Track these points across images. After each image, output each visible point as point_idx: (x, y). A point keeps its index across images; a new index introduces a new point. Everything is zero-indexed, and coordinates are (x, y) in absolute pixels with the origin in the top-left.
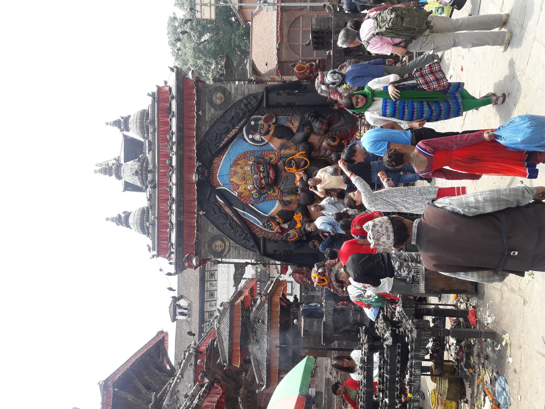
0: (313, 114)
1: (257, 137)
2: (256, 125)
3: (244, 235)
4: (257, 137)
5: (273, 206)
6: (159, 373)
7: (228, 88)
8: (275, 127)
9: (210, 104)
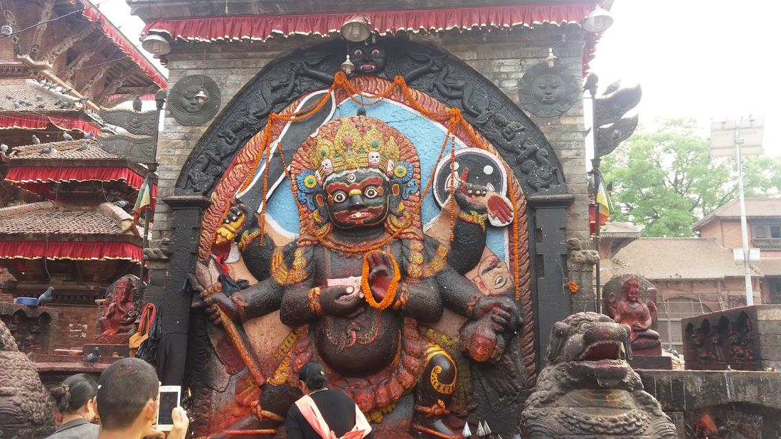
0: (513, 319)
1: (454, 181)
2: (485, 179)
3: (218, 158)
5: (285, 226)
6: (96, 80)
7: (571, 111)
8: (479, 224)
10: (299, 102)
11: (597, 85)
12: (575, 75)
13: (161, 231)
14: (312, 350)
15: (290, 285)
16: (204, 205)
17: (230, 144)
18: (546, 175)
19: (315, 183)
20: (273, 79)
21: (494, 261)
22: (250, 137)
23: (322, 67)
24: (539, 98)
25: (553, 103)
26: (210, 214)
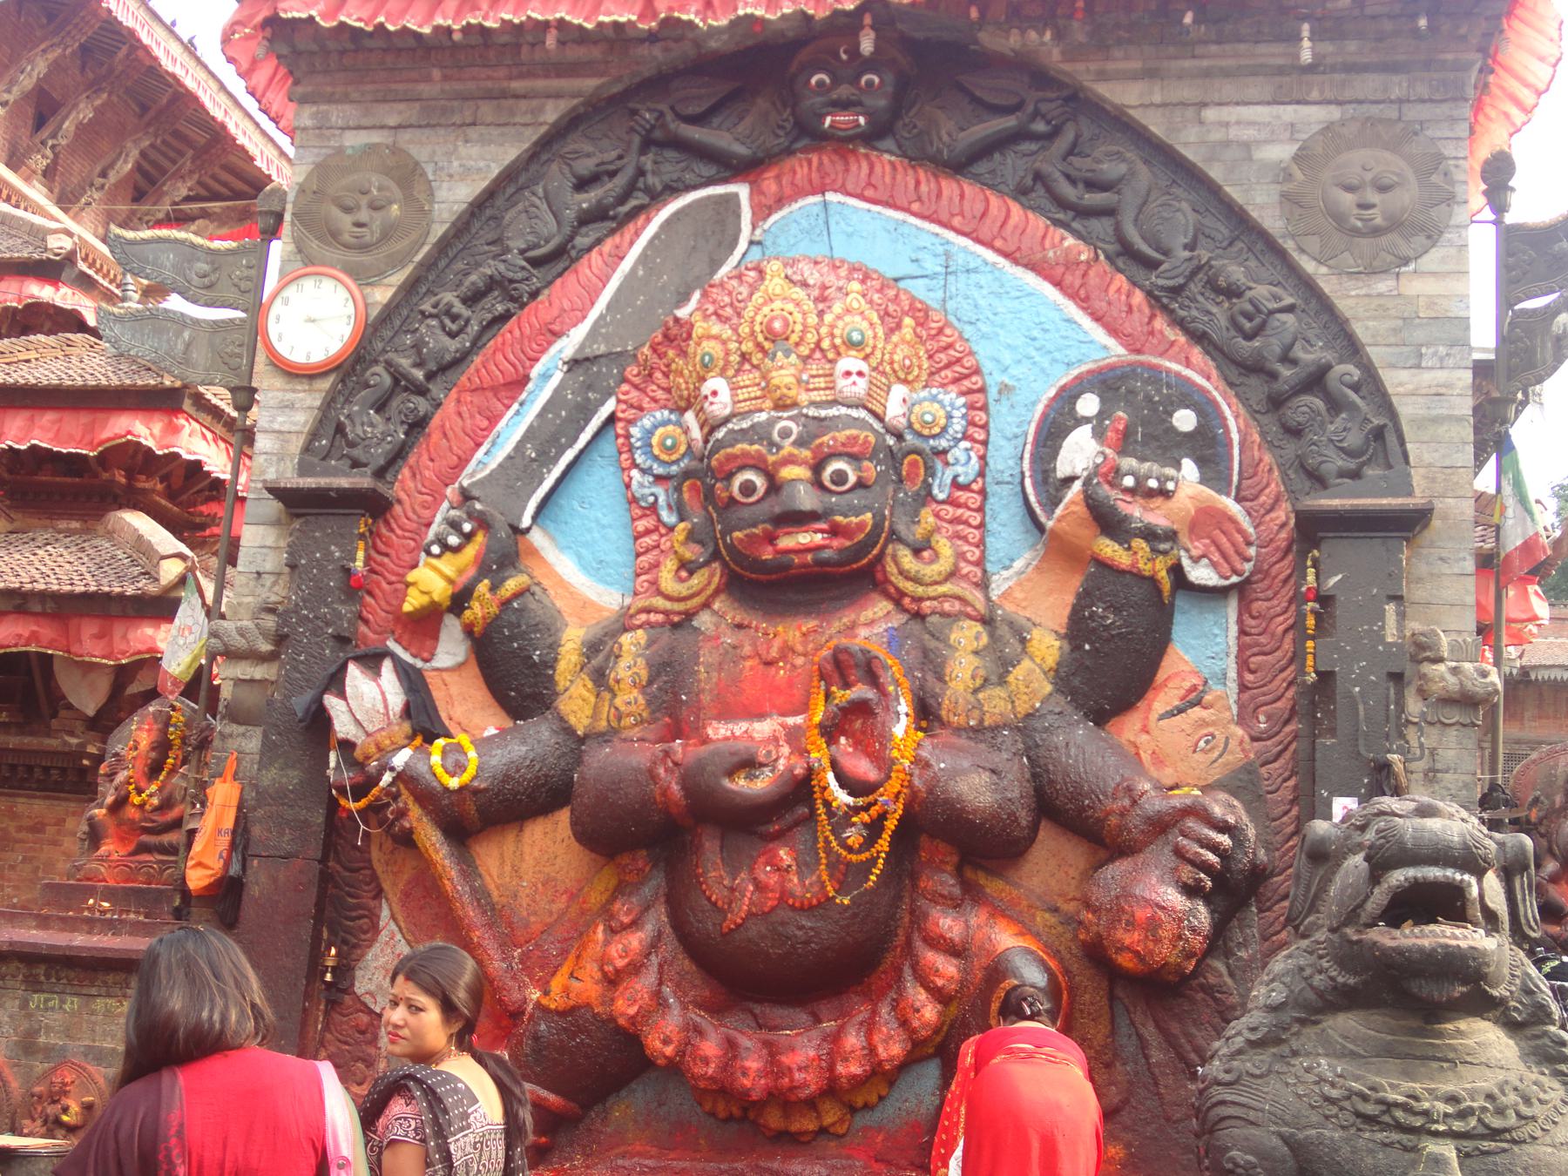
2: (1169, 446)
3: (419, 375)
5: (595, 568)
6: (113, 177)
8: (1153, 581)
9: (1328, 128)
10: (648, 220)
11: (1511, 184)
12: (1446, 153)
13: (258, 573)
14: (657, 918)
15: (601, 735)
17: (452, 335)
18: (1354, 439)
19: (683, 449)
20: (579, 154)
21: (1194, 688)
22: (505, 317)
23: (716, 121)
24: (1339, 218)
25: (1376, 232)
26: (392, 530)
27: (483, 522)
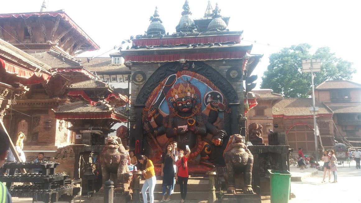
2: (217, 99)
4: (209, 100)
13: (133, 114)
16: (144, 107)
27: (155, 108)
